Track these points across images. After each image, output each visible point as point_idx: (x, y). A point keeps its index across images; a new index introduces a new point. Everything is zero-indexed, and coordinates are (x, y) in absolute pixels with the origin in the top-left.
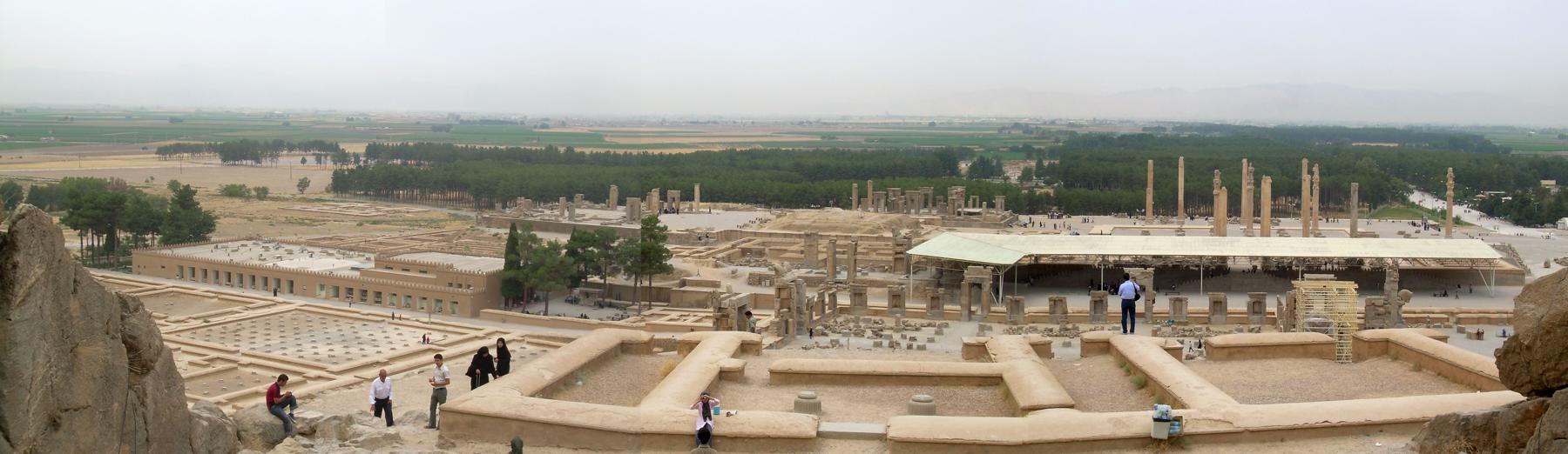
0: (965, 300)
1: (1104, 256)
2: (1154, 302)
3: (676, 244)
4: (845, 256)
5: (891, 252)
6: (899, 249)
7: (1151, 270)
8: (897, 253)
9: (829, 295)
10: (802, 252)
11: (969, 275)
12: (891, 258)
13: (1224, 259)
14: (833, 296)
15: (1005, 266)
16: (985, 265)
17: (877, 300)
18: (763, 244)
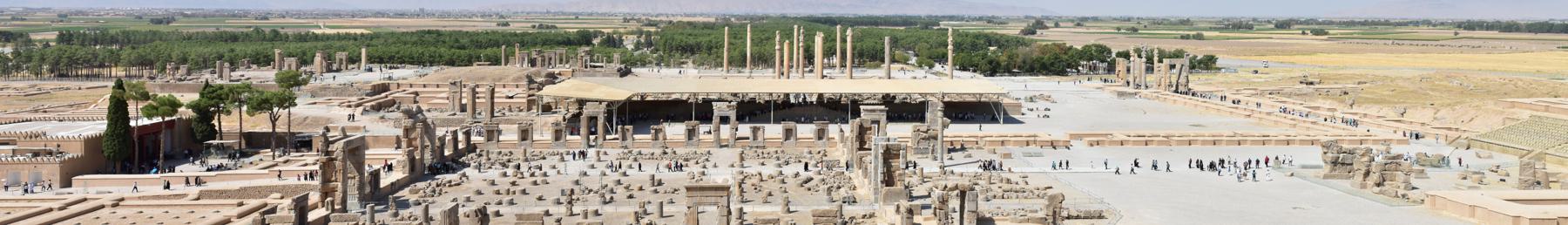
0: (583, 130)
1: (695, 94)
2: (737, 130)
3: (334, 96)
4: (484, 100)
5: (524, 95)
6: (531, 92)
7: (734, 103)
8: (529, 96)
9: (464, 133)
10: (448, 98)
11: (588, 110)
12: (525, 100)
13: (787, 95)
14: (468, 134)
15: (618, 101)
16: (601, 102)
17: (510, 135)
18: (417, 94)
